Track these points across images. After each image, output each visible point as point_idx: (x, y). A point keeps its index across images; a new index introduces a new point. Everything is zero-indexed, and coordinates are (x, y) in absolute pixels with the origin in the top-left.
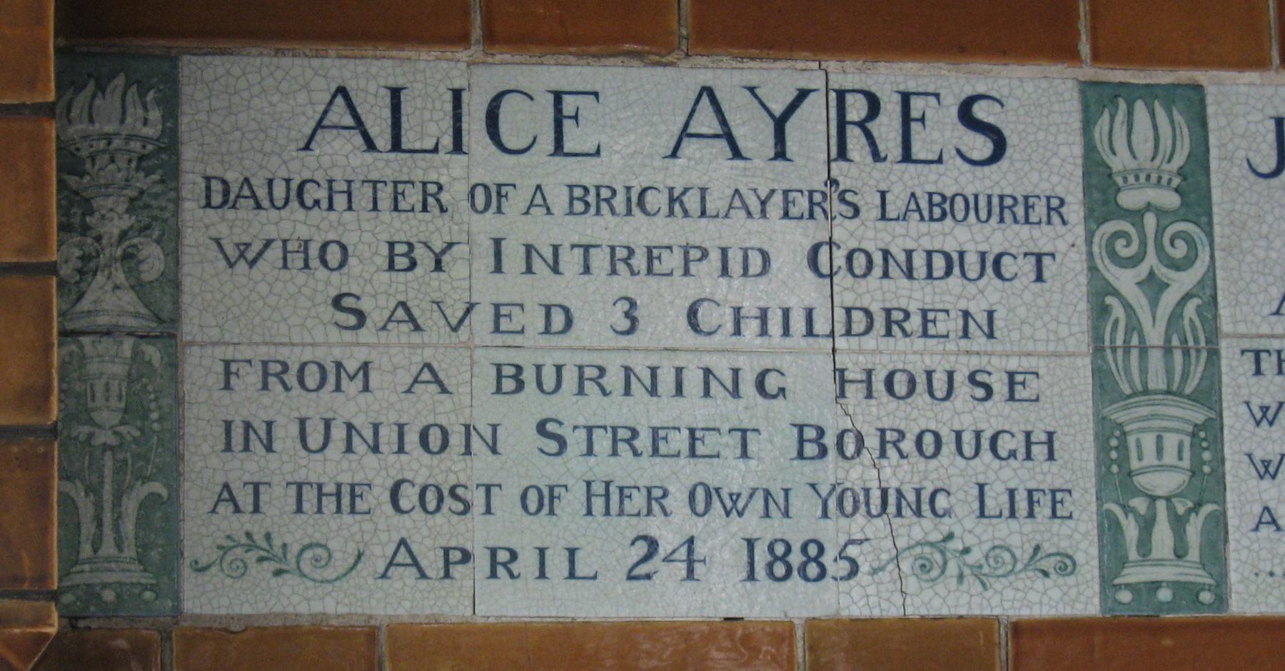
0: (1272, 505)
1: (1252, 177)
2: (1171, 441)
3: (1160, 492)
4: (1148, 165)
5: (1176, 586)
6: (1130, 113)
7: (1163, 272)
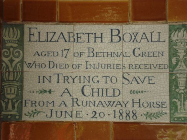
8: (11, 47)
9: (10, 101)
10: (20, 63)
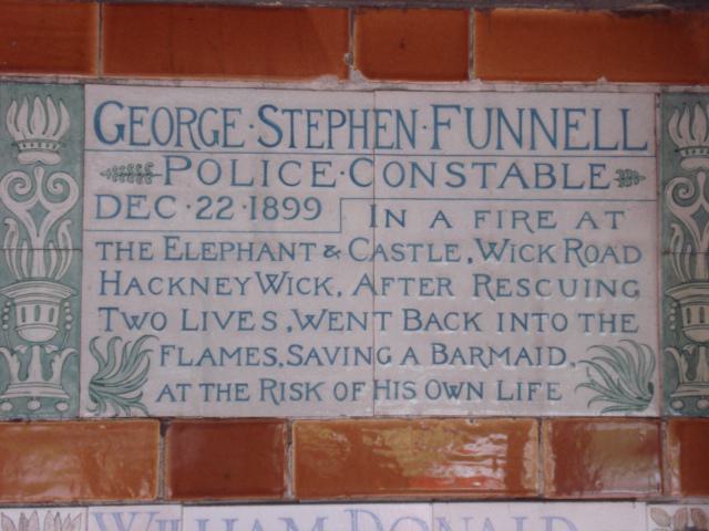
2: (45, 309)
8: (40, 163)
9: (36, 349)
10: (69, 222)
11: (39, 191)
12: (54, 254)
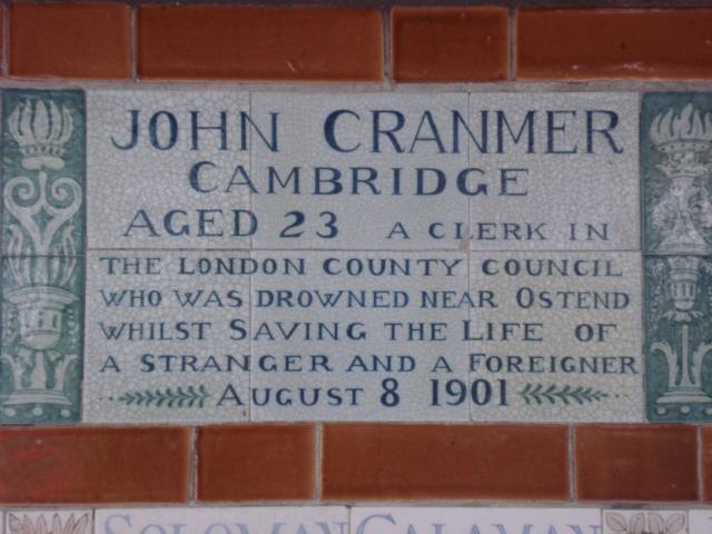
0: (114, 355)
1: (114, 149)
3: (39, 347)
4: (44, 141)
5: (47, 406)
6: (34, 108)
7: (51, 210)
11: (43, 194)
12: (56, 263)
